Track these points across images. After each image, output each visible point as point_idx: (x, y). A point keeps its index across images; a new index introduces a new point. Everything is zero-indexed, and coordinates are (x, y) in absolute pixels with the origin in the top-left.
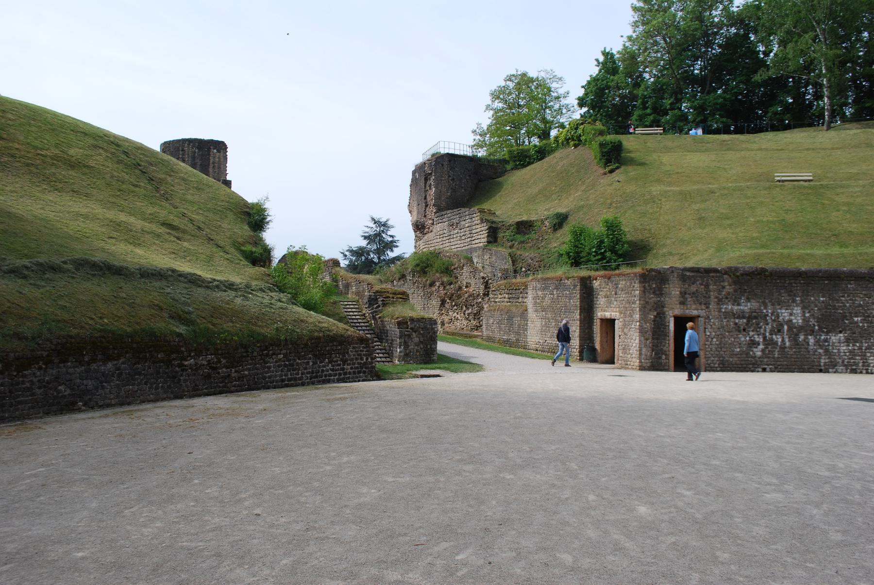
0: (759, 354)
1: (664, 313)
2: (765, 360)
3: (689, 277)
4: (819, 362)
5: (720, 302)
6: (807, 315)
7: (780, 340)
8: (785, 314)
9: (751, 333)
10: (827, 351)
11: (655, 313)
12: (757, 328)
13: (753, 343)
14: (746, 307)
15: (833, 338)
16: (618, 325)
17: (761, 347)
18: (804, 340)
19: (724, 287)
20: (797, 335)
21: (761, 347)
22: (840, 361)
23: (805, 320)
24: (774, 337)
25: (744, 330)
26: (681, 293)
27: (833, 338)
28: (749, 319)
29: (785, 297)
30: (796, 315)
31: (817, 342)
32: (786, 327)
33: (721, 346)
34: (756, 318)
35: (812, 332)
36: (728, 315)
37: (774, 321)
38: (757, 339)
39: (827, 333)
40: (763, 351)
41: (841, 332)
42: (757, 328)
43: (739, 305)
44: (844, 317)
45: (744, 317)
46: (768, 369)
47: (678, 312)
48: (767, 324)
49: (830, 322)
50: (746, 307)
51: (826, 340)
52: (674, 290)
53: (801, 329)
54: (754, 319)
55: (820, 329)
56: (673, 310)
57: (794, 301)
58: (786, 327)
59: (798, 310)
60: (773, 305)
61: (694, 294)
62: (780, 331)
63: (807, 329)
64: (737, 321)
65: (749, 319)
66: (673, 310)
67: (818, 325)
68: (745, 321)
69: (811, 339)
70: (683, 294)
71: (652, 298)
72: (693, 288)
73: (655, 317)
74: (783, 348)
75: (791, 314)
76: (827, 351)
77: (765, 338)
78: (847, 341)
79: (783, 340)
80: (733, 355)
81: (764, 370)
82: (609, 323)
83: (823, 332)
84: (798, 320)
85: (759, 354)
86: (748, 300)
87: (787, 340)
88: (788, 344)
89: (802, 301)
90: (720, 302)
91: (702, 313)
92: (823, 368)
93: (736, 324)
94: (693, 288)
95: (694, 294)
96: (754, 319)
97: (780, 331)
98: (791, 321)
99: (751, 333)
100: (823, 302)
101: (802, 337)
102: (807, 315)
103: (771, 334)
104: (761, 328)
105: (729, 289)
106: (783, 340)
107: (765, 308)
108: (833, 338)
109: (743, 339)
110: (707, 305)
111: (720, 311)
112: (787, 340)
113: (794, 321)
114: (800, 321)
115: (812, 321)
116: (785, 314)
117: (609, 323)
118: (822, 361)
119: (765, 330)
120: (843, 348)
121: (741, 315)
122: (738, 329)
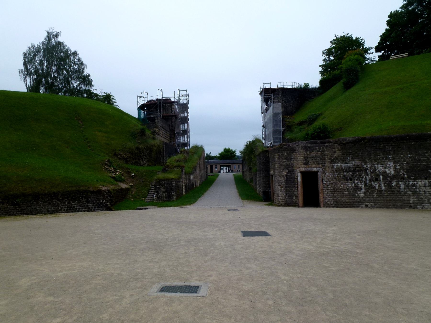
0: (362, 195)
1: (293, 171)
2: (367, 199)
3: (310, 147)
4: (410, 200)
5: (332, 162)
6: (398, 167)
7: (377, 185)
8: (380, 168)
9: (356, 182)
10: (415, 193)
11: (287, 171)
13: (358, 188)
14: (351, 164)
15: (419, 183)
17: (363, 190)
18: (396, 185)
19: (335, 152)
20: (390, 182)
21: (363, 190)
22: (426, 200)
24: (373, 183)
25: (351, 179)
26: (304, 158)
27: (419, 183)
28: (354, 172)
29: (380, 156)
30: (390, 168)
31: (407, 187)
32: (381, 176)
33: (334, 190)
34: (358, 171)
35: (403, 179)
37: (372, 173)
38: (360, 186)
39: (415, 180)
40: (365, 193)
41: (426, 179)
42: (360, 178)
43: (346, 163)
45: (350, 171)
46: (369, 206)
47: (302, 169)
48: (368, 175)
49: (417, 172)
51: (414, 185)
53: (393, 177)
55: (409, 177)
56: (299, 169)
57: (387, 158)
58: (381, 176)
59: (390, 165)
60: (371, 162)
61: (313, 158)
62: (377, 179)
63: (398, 177)
64: (345, 173)
65: (354, 172)
66: (299, 169)
67: (407, 175)
68: (351, 173)
69: (402, 185)
70: (306, 158)
72: (313, 154)
73: (287, 173)
74: (380, 191)
75: (385, 168)
76: (415, 193)
77: (366, 184)
79: (380, 186)
80: (343, 196)
81: (367, 206)
83: (411, 179)
84: (391, 171)
85: (362, 195)
86: (353, 159)
87: (383, 185)
88: (383, 188)
89: (393, 158)
90: (332, 162)
91: (320, 170)
92: (412, 205)
93: (344, 176)
94: (313, 154)
95: (313, 158)
96: (357, 173)
97: (377, 179)
98: (386, 172)
99: (356, 182)
100: (410, 157)
101: (394, 183)
102: (398, 167)
103: (370, 181)
104: (363, 177)
105: (338, 153)
106: (380, 186)
107: (365, 164)
108: (420, 183)
109: (350, 185)
110: (323, 164)
111: (332, 167)
112: (383, 185)
113: (388, 172)
114: (393, 172)
115: (402, 172)
116: (380, 168)
118: (412, 200)
119: (366, 179)
121: (348, 170)
122: (346, 179)
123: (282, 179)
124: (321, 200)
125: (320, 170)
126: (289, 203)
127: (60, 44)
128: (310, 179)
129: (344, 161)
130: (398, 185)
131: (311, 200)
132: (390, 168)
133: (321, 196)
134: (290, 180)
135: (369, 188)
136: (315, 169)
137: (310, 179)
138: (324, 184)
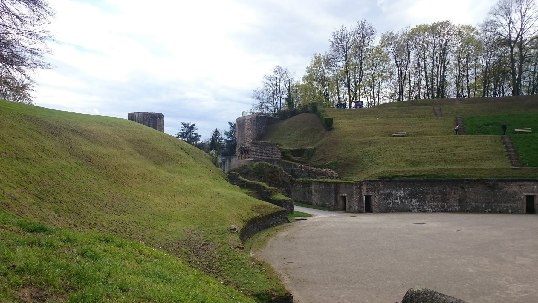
8: (398, 194)
12: (390, 198)
13: (389, 203)
14: (386, 191)
16: (347, 198)
23: (404, 195)
28: (388, 195)
31: (408, 202)
33: (379, 204)
36: (382, 194)
42: (390, 198)
44: (416, 194)
47: (366, 194)
49: (412, 196)
50: (386, 191)
52: (365, 188)
53: (403, 198)
54: (389, 195)
56: (365, 193)
59: (402, 192)
61: (370, 189)
62: (397, 199)
65: (388, 195)
66: (365, 193)
70: (367, 189)
71: (359, 190)
72: (370, 187)
74: (398, 204)
78: (418, 201)
80: (383, 207)
82: (344, 198)
84: (402, 195)
86: (387, 190)
90: (379, 190)
94: (370, 187)
95: (370, 189)
97: (397, 199)
105: (381, 186)
108: (414, 201)
110: (375, 192)
116: (398, 194)
117: (344, 198)
122: (385, 199)
123: (357, 199)
125: (373, 194)
126: (360, 212)
131: (369, 210)
135: (394, 203)
138: (374, 202)
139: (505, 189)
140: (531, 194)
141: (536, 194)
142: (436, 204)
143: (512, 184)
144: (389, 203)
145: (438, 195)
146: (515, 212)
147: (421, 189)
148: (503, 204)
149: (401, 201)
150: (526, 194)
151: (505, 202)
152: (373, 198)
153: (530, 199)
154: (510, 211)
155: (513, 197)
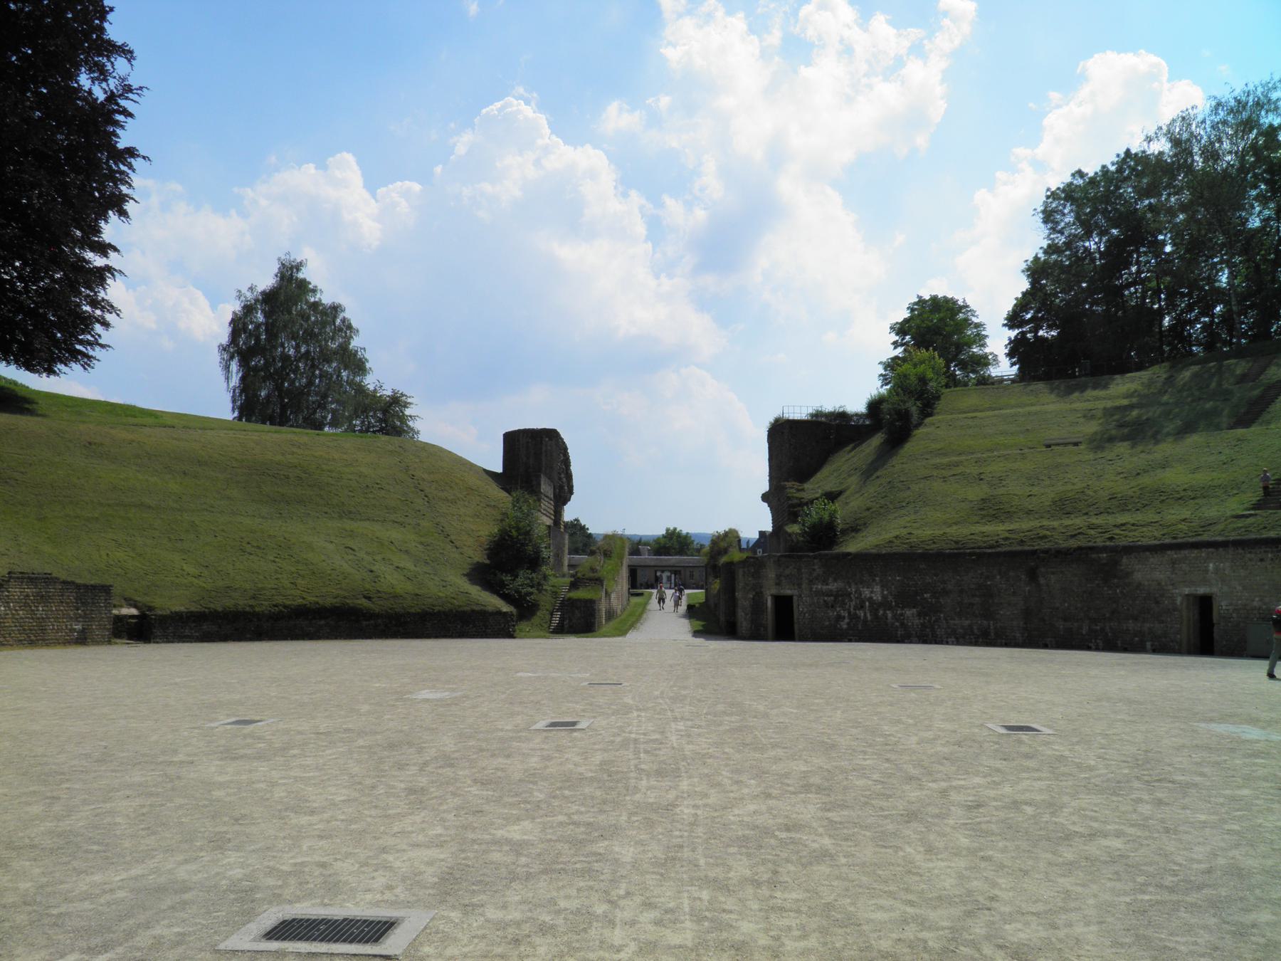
8: (866, 592)
10: (902, 624)
13: (840, 618)
14: (833, 586)
21: (847, 620)
23: (884, 597)
28: (836, 596)
30: (875, 592)
31: (894, 616)
35: (890, 608)
39: (902, 608)
47: (774, 591)
49: (905, 598)
50: (833, 586)
52: (771, 573)
53: (880, 605)
54: (840, 597)
55: (897, 605)
59: (877, 589)
62: (862, 607)
63: (885, 604)
65: (836, 596)
69: (889, 614)
70: (778, 577)
72: (787, 572)
74: (865, 621)
78: (919, 615)
84: (877, 597)
86: (835, 580)
90: (811, 582)
94: (787, 572)
97: (862, 607)
105: (819, 571)
108: (908, 612)
110: (799, 585)
115: (890, 598)
116: (866, 592)
120: (917, 621)
121: (829, 594)
123: (747, 604)
124: (797, 631)
127: (303, 285)
128: (784, 604)
129: (825, 582)
130: (885, 615)
132: (875, 592)
133: (796, 627)
134: (758, 606)
135: (853, 617)
136: (788, 592)
137: (784, 604)
138: (801, 610)
139: (1138, 576)
140: (1202, 590)
141: (1214, 590)
142: (967, 623)
143: (1154, 560)
144: (840, 618)
145: (973, 596)
146: (1163, 646)
147: (928, 580)
148: (1131, 625)
149: (874, 611)
150: (1187, 591)
151: (1136, 619)
152: (795, 598)
153: (1205, 604)
154: (1148, 645)
155: (1157, 603)
